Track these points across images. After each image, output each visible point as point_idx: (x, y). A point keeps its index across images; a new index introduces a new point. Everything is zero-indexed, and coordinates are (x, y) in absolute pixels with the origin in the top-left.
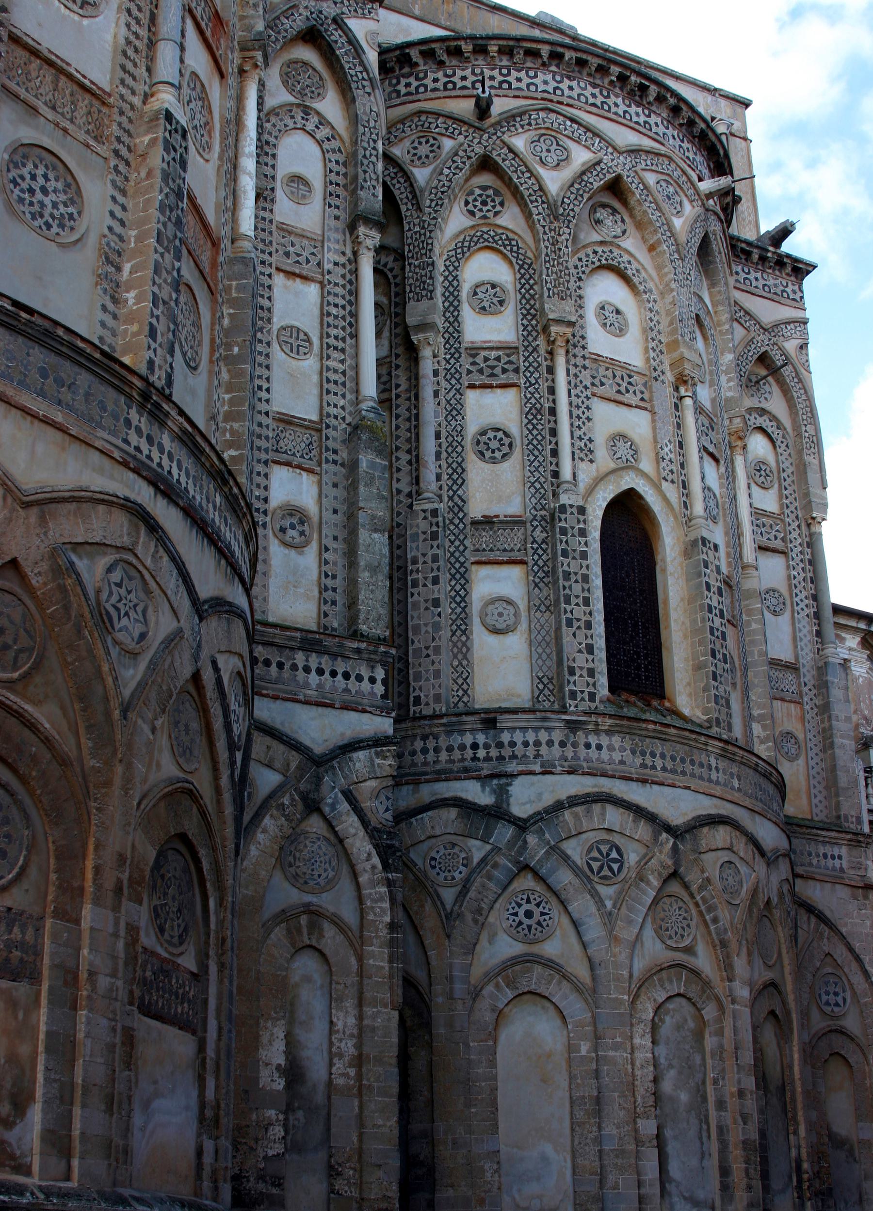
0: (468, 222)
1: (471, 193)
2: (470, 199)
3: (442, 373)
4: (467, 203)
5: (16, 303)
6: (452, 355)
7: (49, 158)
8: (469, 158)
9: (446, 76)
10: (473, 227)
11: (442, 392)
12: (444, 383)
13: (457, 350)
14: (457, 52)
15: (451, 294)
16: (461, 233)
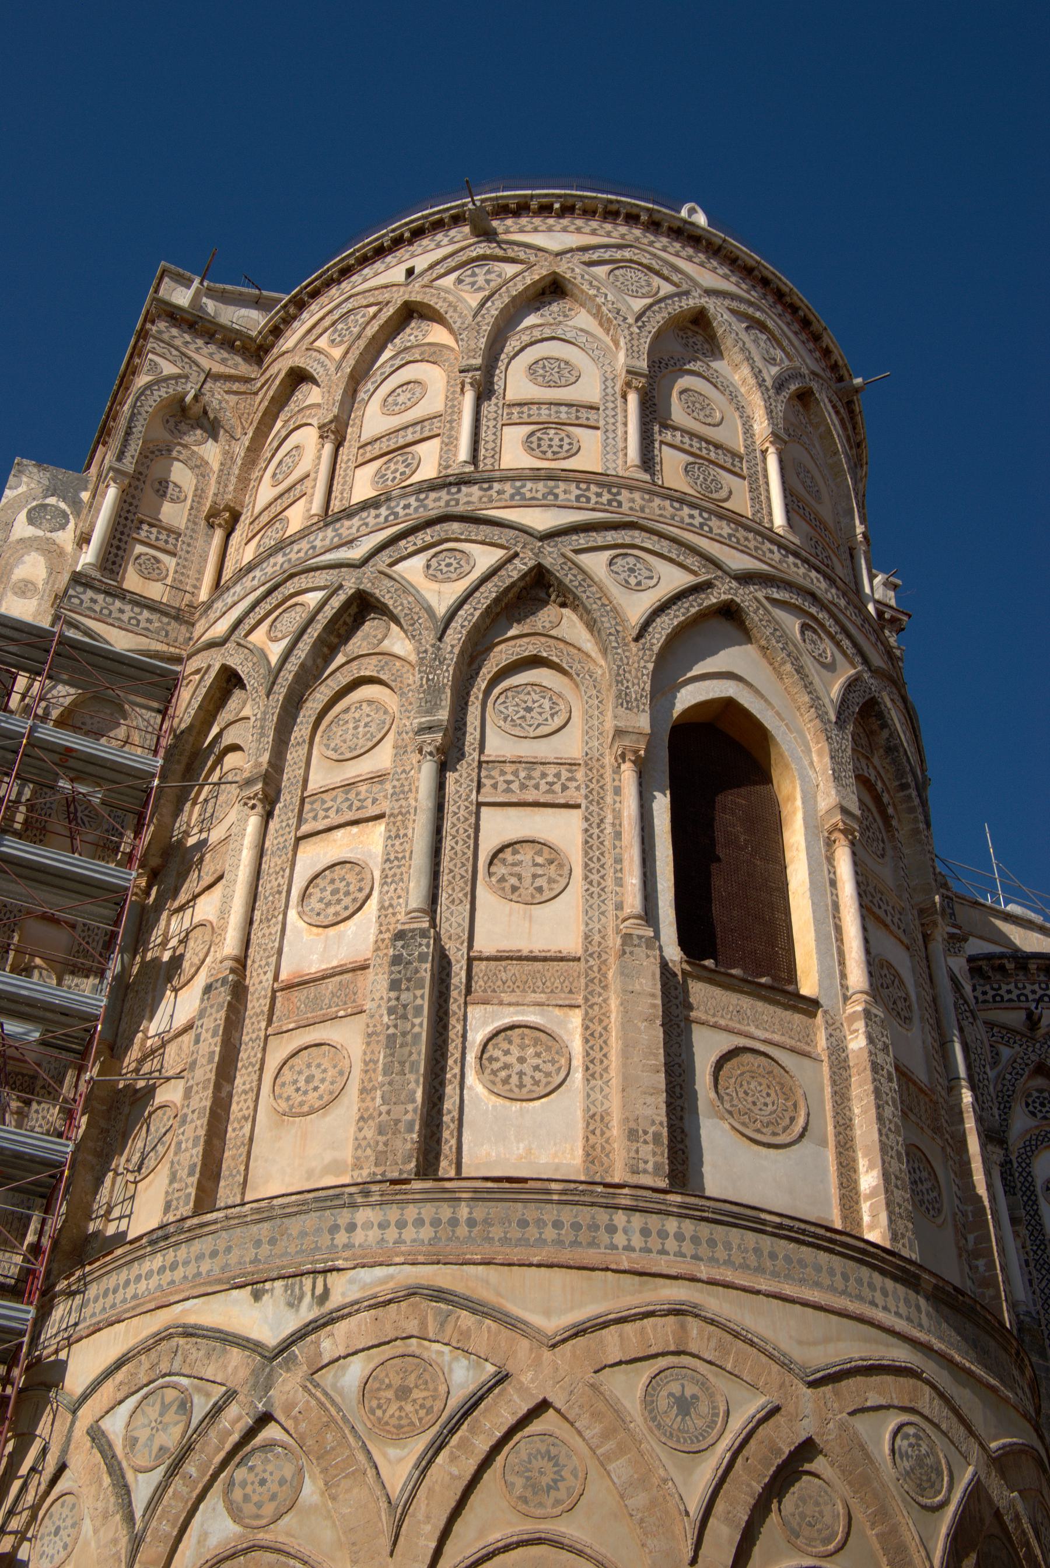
0: (1031, 1122)
1: (1030, 1095)
2: (1030, 1101)
3: (1032, 1264)
4: (1027, 1105)
5: (955, 1289)
6: (1039, 1247)
7: (919, 1154)
8: (1027, 1065)
9: (993, 989)
10: (1037, 1127)
11: (1035, 1282)
12: (1034, 1273)
13: (1042, 1242)
14: (1002, 968)
15: (1028, 1189)
16: (1027, 1131)
